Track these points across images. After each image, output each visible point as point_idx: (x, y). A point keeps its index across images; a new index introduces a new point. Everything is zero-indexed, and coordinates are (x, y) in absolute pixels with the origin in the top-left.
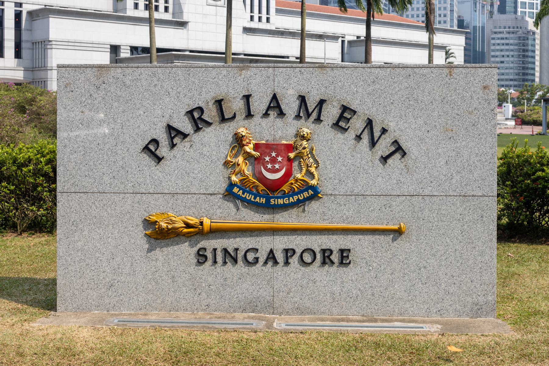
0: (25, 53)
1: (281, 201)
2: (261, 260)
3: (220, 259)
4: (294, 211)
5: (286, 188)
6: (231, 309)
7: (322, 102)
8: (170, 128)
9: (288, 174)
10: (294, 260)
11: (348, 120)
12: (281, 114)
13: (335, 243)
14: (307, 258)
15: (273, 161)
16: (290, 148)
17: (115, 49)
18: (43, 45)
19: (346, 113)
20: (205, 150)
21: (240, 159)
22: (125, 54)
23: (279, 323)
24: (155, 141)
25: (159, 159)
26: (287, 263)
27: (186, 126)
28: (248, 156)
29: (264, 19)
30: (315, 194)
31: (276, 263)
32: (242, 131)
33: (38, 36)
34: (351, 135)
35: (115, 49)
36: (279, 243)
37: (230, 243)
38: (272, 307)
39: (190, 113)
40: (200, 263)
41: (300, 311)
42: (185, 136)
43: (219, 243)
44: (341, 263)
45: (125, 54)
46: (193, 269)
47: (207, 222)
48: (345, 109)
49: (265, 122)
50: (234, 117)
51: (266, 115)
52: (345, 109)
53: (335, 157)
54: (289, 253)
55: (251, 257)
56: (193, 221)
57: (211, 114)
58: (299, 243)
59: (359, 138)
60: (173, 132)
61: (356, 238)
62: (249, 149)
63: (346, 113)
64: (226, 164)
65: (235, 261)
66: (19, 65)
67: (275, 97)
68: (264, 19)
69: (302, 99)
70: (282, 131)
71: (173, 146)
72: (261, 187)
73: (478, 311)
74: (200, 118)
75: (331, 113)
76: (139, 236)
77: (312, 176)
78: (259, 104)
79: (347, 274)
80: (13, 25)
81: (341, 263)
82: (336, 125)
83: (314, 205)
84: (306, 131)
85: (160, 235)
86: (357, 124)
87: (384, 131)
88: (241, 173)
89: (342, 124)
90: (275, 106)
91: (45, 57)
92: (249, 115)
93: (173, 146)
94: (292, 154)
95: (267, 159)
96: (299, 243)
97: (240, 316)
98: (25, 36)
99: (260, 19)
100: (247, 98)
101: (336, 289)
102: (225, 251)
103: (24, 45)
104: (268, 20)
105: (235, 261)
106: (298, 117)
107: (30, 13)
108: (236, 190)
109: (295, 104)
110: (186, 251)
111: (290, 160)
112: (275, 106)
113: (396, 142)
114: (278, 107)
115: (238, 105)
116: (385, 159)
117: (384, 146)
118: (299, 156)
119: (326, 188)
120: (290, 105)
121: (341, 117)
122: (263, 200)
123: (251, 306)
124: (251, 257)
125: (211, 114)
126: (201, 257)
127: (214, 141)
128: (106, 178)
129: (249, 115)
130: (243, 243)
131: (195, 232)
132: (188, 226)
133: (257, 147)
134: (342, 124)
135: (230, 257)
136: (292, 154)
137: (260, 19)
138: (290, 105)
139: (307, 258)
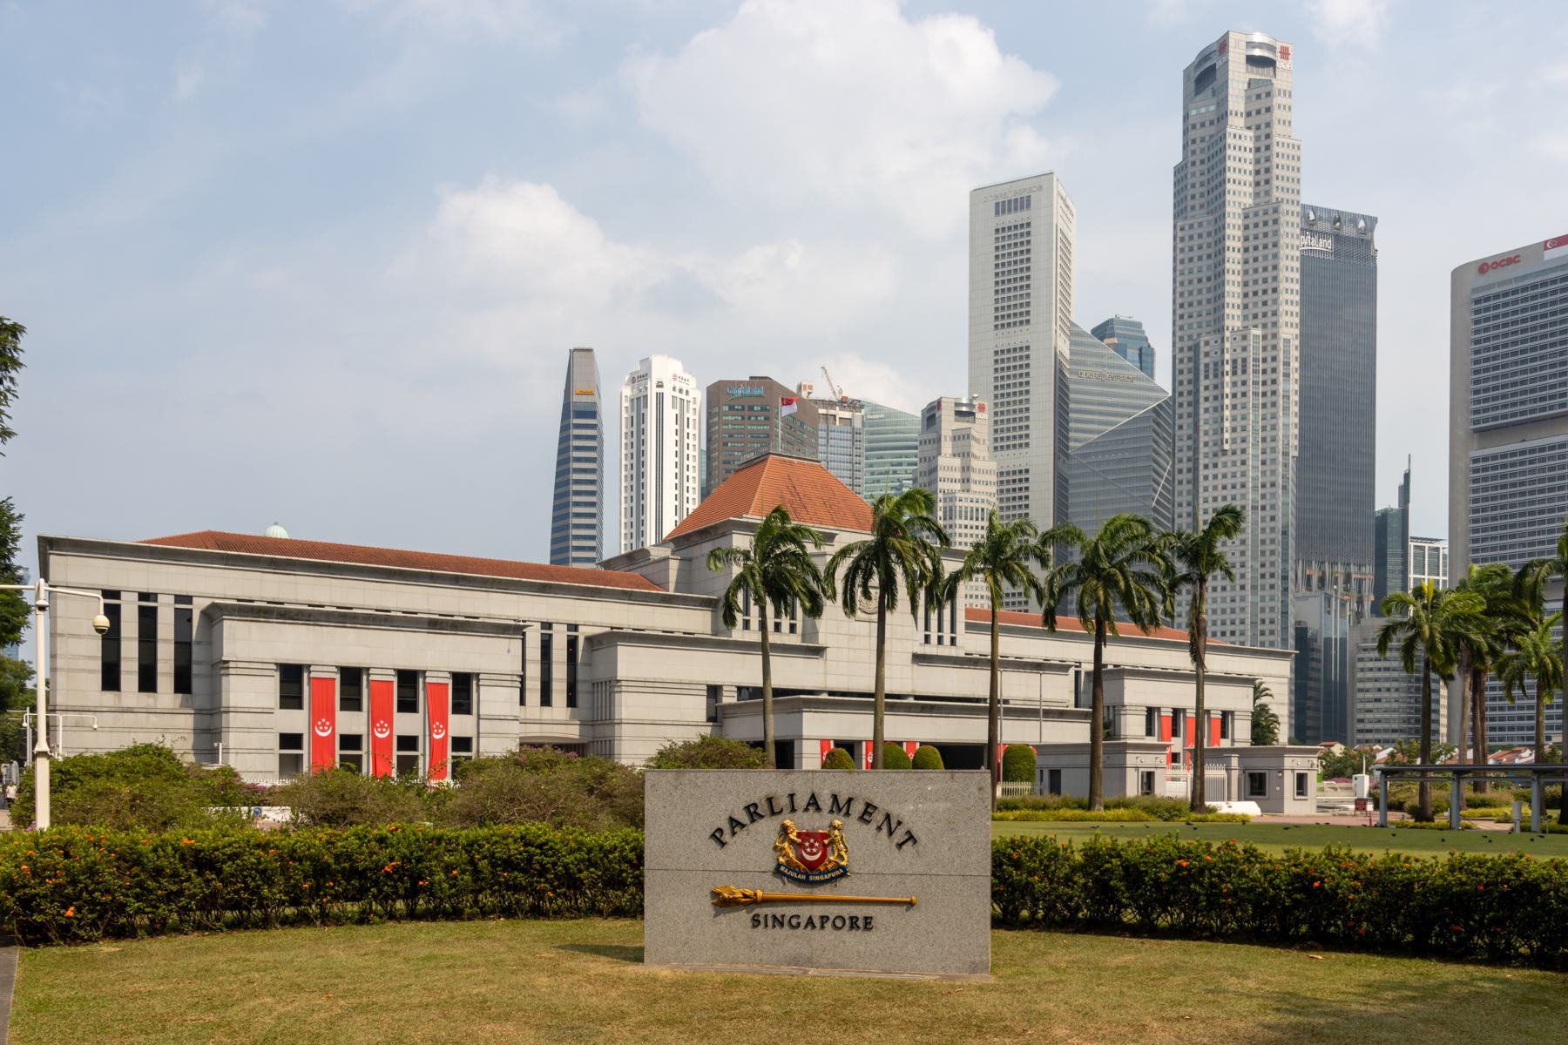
0: (582, 699)
3: (770, 923)
4: (828, 886)
6: (779, 963)
8: (731, 820)
9: (824, 856)
10: (828, 925)
12: (818, 809)
13: (860, 912)
14: (839, 923)
15: (812, 846)
16: (825, 836)
17: (714, 691)
18: (608, 686)
19: (869, 808)
20: (759, 837)
21: (786, 845)
22: (729, 698)
23: (812, 972)
24: (720, 830)
25: (723, 844)
26: (822, 927)
27: (744, 819)
28: (792, 842)
30: (844, 873)
32: (788, 822)
33: (601, 674)
34: (873, 826)
35: (714, 691)
36: (817, 911)
37: (779, 911)
38: (810, 962)
39: (747, 808)
40: (754, 926)
41: (833, 965)
42: (743, 826)
43: (768, 911)
46: (749, 931)
47: (760, 893)
48: (868, 805)
49: (805, 815)
51: (806, 810)
52: (868, 805)
53: (859, 844)
54: (824, 919)
55: (794, 922)
56: (749, 892)
57: (763, 808)
58: (832, 911)
59: (879, 828)
60: (734, 823)
61: (877, 908)
62: (793, 836)
63: (869, 808)
64: (775, 848)
65: (782, 924)
66: (573, 717)
67: (813, 796)
69: (835, 798)
70: (818, 822)
71: (734, 834)
73: (974, 968)
75: (858, 808)
76: (707, 903)
77: (842, 858)
78: (801, 801)
79: (871, 936)
80: (565, 658)
82: (861, 818)
83: (844, 882)
84: (837, 822)
85: (724, 903)
86: (878, 817)
88: (786, 855)
90: (814, 802)
91: (610, 704)
92: (793, 810)
93: (734, 834)
94: (825, 840)
96: (832, 911)
97: (784, 968)
100: (792, 796)
101: (862, 948)
102: (774, 917)
103: (580, 687)
105: (782, 924)
106: (831, 811)
107: (589, 639)
109: (829, 802)
110: (744, 916)
111: (825, 846)
112: (814, 802)
114: (816, 803)
115: (785, 802)
116: (900, 846)
117: (899, 835)
118: (832, 842)
119: (854, 868)
120: (825, 803)
121: (865, 812)
123: (795, 961)
124: (794, 922)
125: (763, 808)
126: (756, 922)
127: (767, 829)
128: (683, 859)
129: (793, 810)
130: (789, 911)
131: (751, 902)
132: (745, 896)
133: (799, 835)
135: (778, 921)
136: (825, 840)
138: (825, 803)
139: (839, 923)
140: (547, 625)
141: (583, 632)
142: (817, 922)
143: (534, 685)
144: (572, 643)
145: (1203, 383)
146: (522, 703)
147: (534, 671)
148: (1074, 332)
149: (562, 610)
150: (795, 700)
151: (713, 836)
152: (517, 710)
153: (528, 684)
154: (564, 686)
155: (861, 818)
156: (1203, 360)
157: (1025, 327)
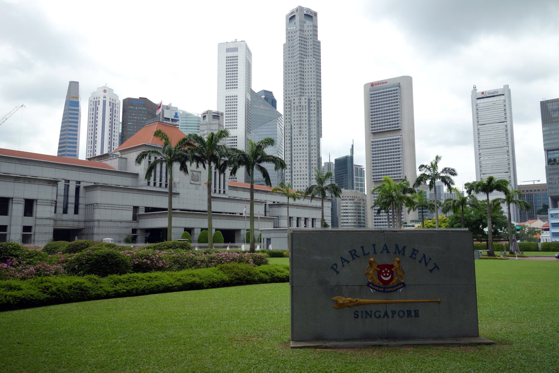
0: (81, 211)
1: (390, 290)
2: (382, 316)
5: (391, 284)
7: (404, 248)
8: (342, 258)
11: (416, 255)
14: (401, 314)
17: (136, 208)
22: (142, 212)
25: (338, 273)
26: (393, 317)
29: (222, 192)
31: (388, 317)
35: (136, 208)
39: (350, 252)
42: (348, 262)
44: (415, 316)
45: (142, 212)
50: (369, 253)
52: (414, 250)
54: (394, 312)
55: (377, 315)
59: (420, 262)
63: (415, 252)
65: (371, 316)
68: (222, 192)
69: (397, 246)
71: (343, 266)
72: (381, 284)
74: (355, 254)
75: (408, 253)
78: (380, 247)
81: (415, 316)
82: (411, 257)
86: (419, 256)
87: (430, 259)
89: (414, 256)
95: (383, 271)
98: (81, 201)
99: (220, 191)
100: (374, 245)
102: (367, 312)
103: (80, 206)
104: (224, 192)
105: (371, 316)
107: (86, 188)
108: (371, 285)
113: (435, 264)
116: (431, 271)
117: (431, 266)
121: (413, 253)
122: (382, 289)
124: (377, 315)
129: (375, 253)
134: (414, 256)
137: (220, 191)
138: (392, 249)
140: (68, 181)
141: (82, 185)
142: (390, 314)
143: (60, 205)
144: (77, 189)
145: (293, 112)
146: (55, 212)
147: (61, 199)
148: (252, 92)
149: (74, 176)
150: (168, 212)
151: (332, 268)
152: (53, 215)
153: (58, 205)
154: (73, 206)
155: (411, 257)
156: (293, 105)
157: (236, 89)
